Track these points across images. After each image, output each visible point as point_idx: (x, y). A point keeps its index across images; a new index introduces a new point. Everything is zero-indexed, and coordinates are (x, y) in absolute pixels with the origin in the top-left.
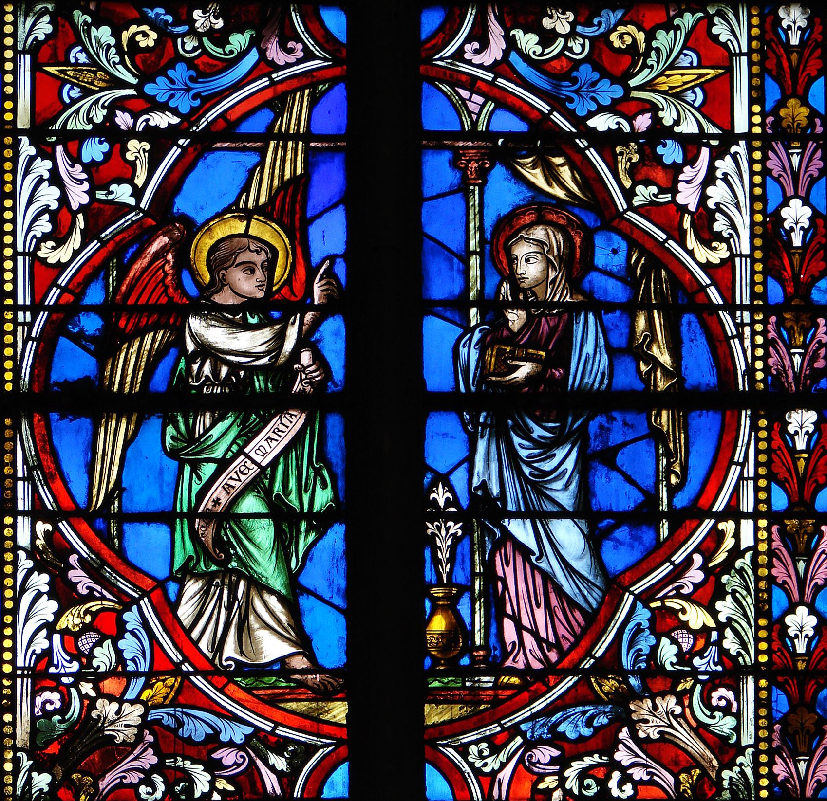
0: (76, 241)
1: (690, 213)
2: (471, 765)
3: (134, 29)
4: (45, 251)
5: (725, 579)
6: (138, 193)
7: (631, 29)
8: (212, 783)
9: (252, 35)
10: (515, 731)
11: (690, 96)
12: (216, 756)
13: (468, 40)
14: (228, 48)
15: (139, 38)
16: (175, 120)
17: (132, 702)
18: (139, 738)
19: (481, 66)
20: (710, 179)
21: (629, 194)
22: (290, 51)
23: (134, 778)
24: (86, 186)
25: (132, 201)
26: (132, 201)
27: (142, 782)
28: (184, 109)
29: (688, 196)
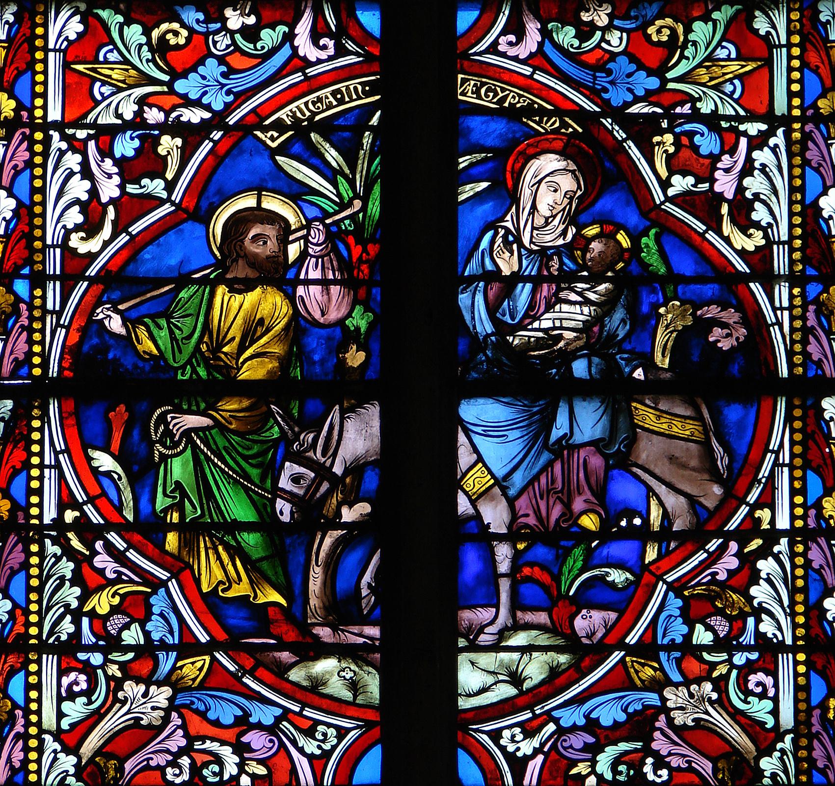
0: (107, 232)
1: (727, 200)
2: (503, 749)
3: (164, 27)
4: (75, 241)
5: (761, 564)
6: (170, 187)
7: (669, 21)
8: (241, 766)
9: (285, 32)
10: (549, 717)
11: (728, 88)
12: (245, 739)
13: (504, 32)
14: (259, 45)
15: (169, 36)
16: (207, 115)
17: (159, 684)
18: (166, 720)
19: (515, 59)
20: (748, 169)
21: (665, 185)
22: (324, 48)
23: (160, 760)
24: (116, 180)
25: (164, 195)
26: (164, 195)
27: (170, 764)
28: (218, 106)
29: (725, 184)
